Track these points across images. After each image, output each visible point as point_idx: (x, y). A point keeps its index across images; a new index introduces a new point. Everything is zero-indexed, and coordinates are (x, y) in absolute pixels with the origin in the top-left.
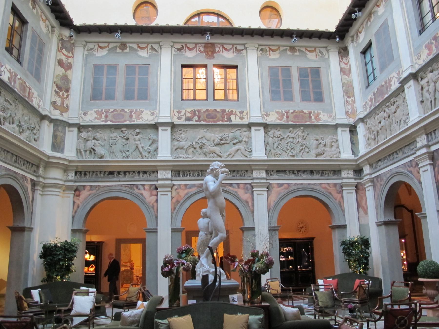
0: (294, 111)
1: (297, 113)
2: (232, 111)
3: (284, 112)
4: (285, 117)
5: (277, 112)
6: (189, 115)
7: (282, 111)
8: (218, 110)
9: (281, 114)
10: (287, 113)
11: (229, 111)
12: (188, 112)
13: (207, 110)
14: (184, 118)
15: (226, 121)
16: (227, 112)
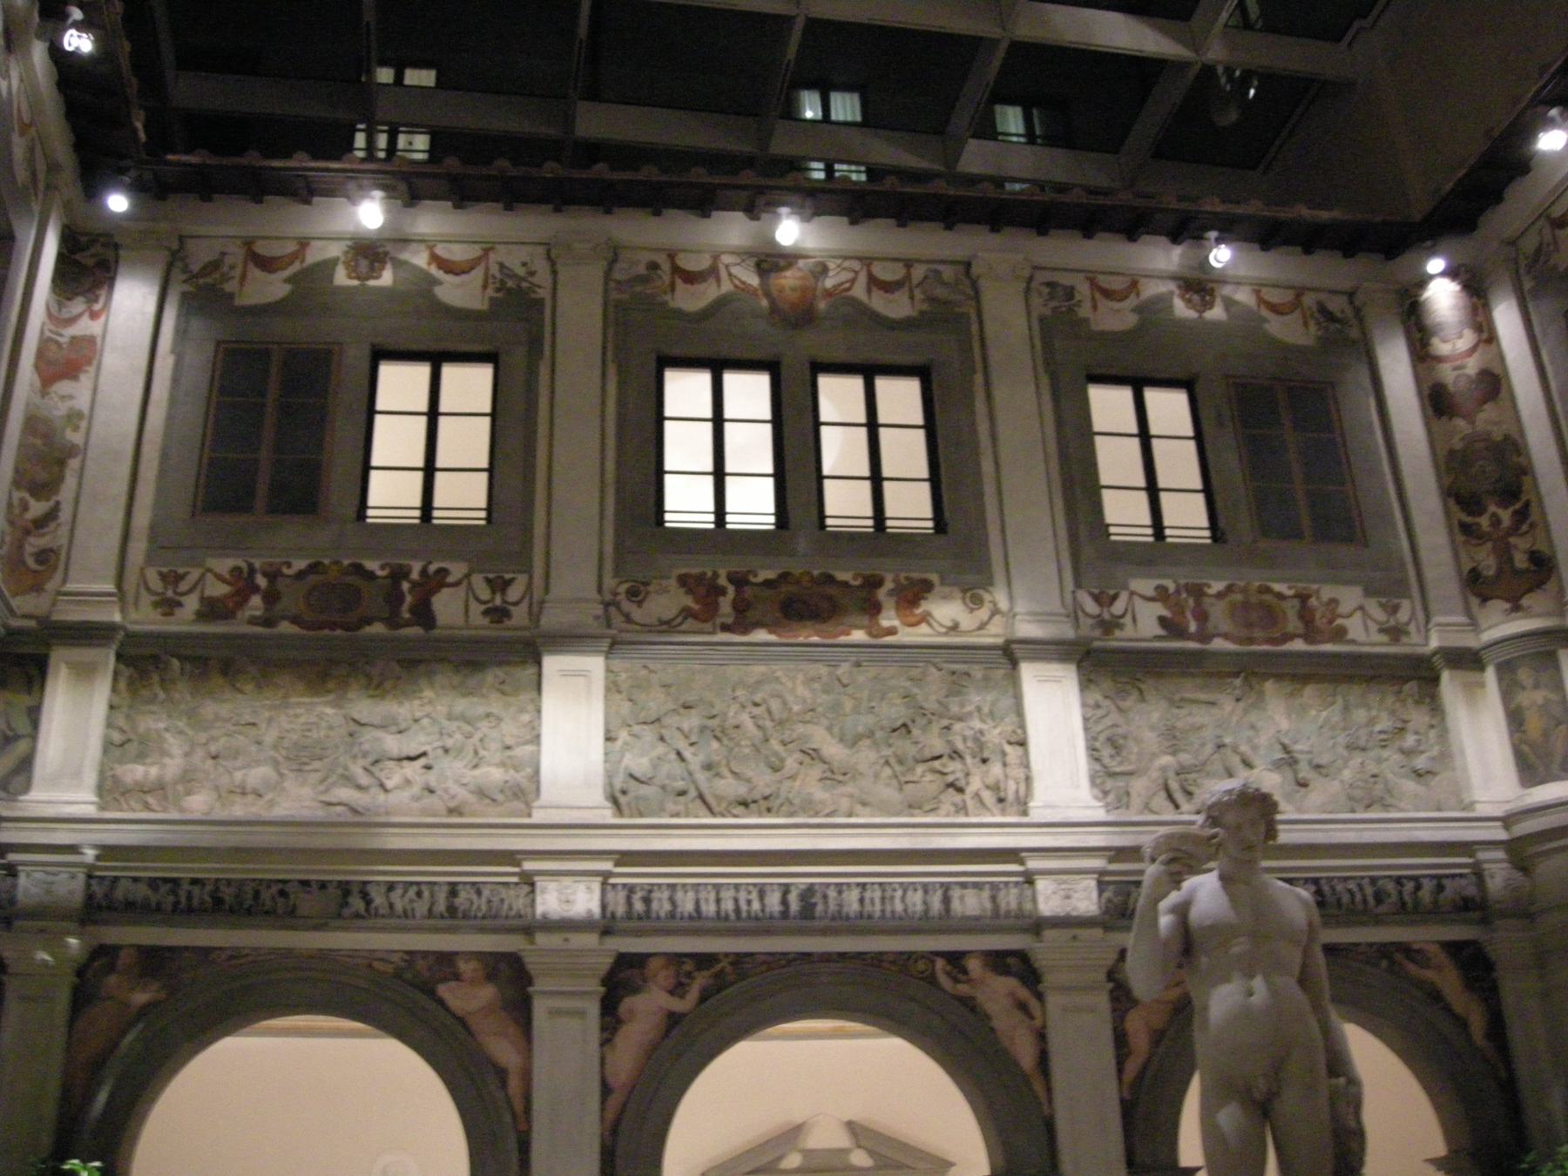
0: (785, 577)
1: (792, 589)
2: (443, 572)
3: (722, 581)
4: (726, 605)
5: (683, 581)
6: (217, 589)
7: (716, 575)
8: (372, 565)
9: (702, 590)
10: (739, 581)
11: (424, 572)
12: (219, 577)
13: (314, 568)
14: (192, 604)
15: (408, 624)
16: (415, 575)
